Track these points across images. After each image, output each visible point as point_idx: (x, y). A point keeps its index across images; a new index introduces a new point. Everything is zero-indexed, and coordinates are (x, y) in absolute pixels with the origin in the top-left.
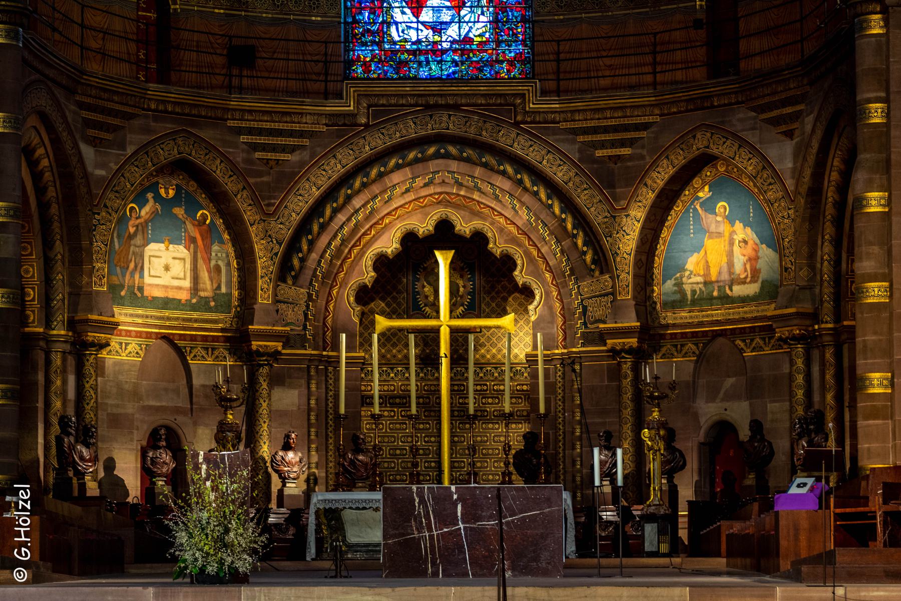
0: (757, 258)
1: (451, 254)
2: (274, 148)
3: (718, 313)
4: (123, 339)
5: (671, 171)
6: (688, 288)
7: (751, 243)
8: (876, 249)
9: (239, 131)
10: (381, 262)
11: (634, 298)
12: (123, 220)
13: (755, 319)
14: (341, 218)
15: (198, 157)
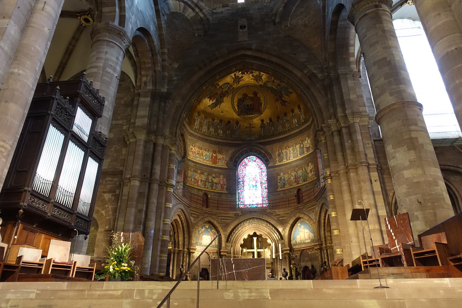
0: (310, 235)
1: (256, 238)
2: (225, 219)
3: (303, 246)
4: (198, 252)
5: (293, 221)
6: (297, 242)
7: (308, 232)
8: (335, 224)
9: (219, 216)
10: (244, 240)
11: (288, 244)
12: (199, 231)
13: (310, 246)
14: (237, 231)
15: (212, 220)
